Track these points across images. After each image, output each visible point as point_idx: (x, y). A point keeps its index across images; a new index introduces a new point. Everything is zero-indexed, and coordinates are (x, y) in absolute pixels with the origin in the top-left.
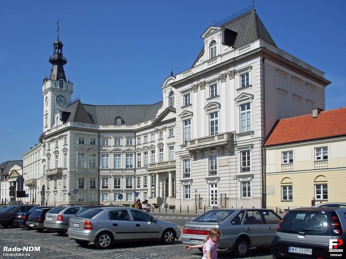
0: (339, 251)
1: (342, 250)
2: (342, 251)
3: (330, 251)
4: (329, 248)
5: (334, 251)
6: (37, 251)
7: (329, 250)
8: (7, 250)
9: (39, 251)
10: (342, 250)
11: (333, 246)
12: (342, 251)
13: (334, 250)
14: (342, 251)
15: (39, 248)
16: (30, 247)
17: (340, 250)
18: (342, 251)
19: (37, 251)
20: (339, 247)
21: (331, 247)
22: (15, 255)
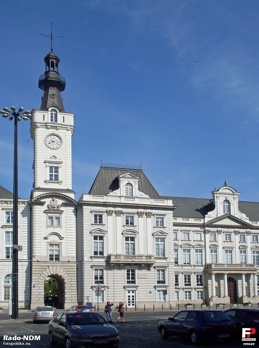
0: (252, 340)
1: (255, 339)
2: (254, 339)
3: (243, 340)
4: (242, 337)
5: (247, 340)
6: (37, 340)
7: (242, 339)
8: (8, 338)
9: (39, 340)
10: (255, 339)
11: (246, 335)
12: (255, 340)
13: (247, 339)
14: (254, 339)
15: (39, 337)
16: (30, 336)
17: (253, 339)
18: (255, 340)
19: (37, 340)
20: (251, 336)
21: (244, 336)
22: (15, 344)
